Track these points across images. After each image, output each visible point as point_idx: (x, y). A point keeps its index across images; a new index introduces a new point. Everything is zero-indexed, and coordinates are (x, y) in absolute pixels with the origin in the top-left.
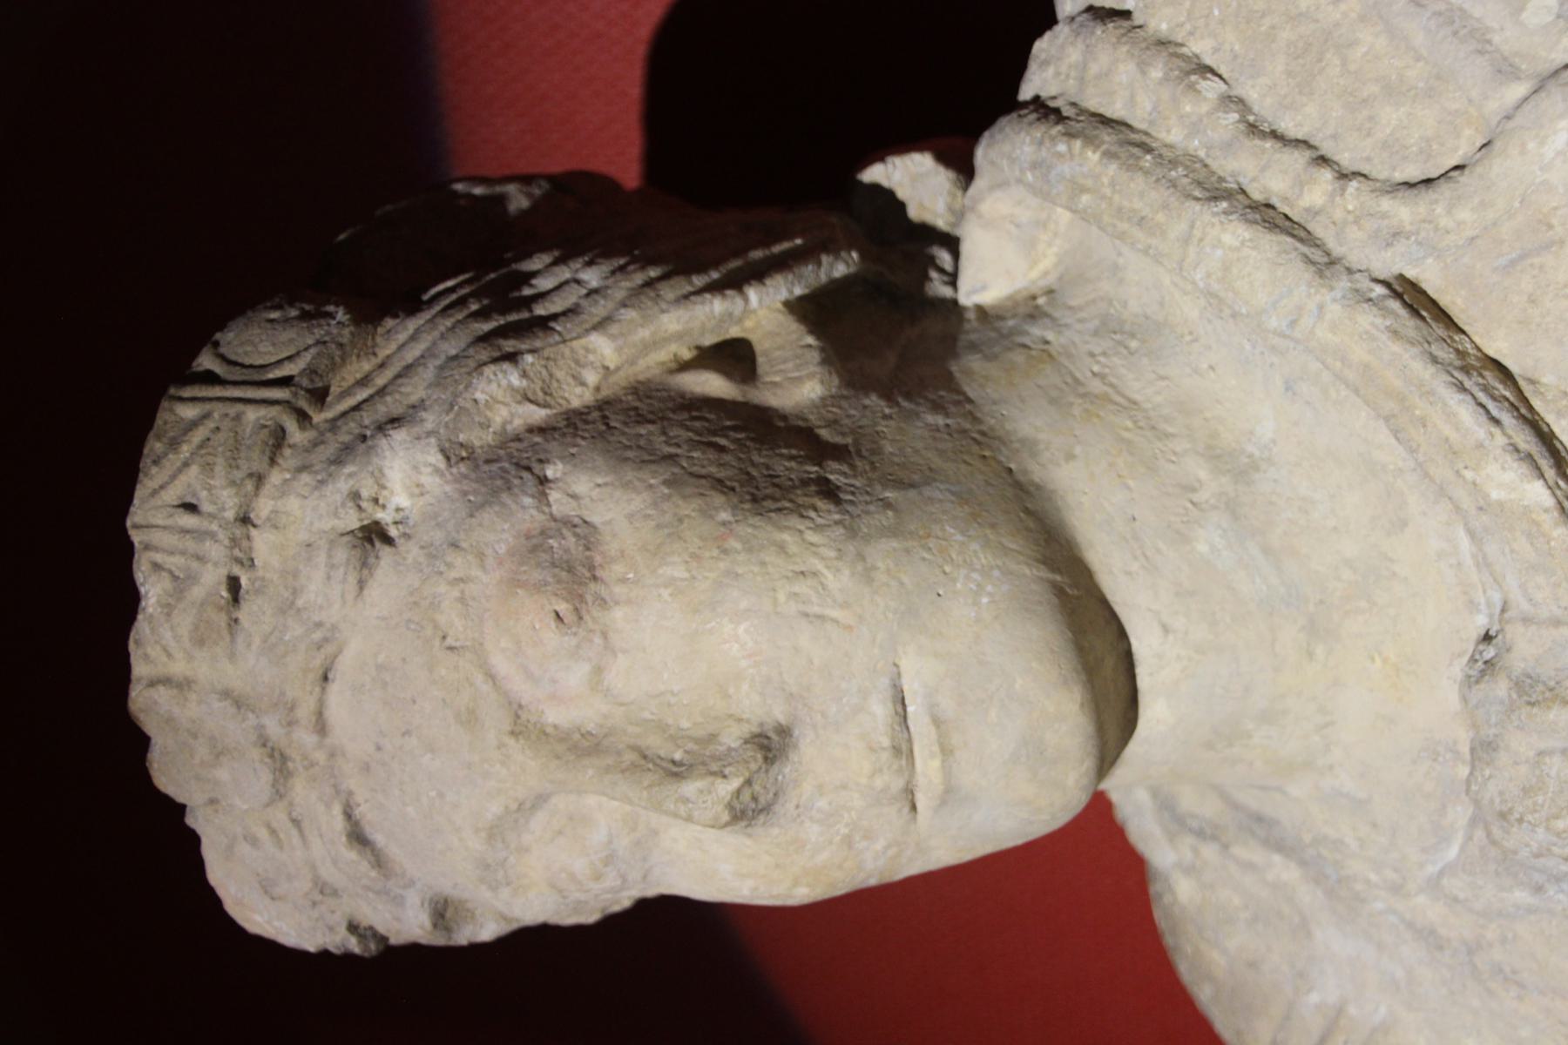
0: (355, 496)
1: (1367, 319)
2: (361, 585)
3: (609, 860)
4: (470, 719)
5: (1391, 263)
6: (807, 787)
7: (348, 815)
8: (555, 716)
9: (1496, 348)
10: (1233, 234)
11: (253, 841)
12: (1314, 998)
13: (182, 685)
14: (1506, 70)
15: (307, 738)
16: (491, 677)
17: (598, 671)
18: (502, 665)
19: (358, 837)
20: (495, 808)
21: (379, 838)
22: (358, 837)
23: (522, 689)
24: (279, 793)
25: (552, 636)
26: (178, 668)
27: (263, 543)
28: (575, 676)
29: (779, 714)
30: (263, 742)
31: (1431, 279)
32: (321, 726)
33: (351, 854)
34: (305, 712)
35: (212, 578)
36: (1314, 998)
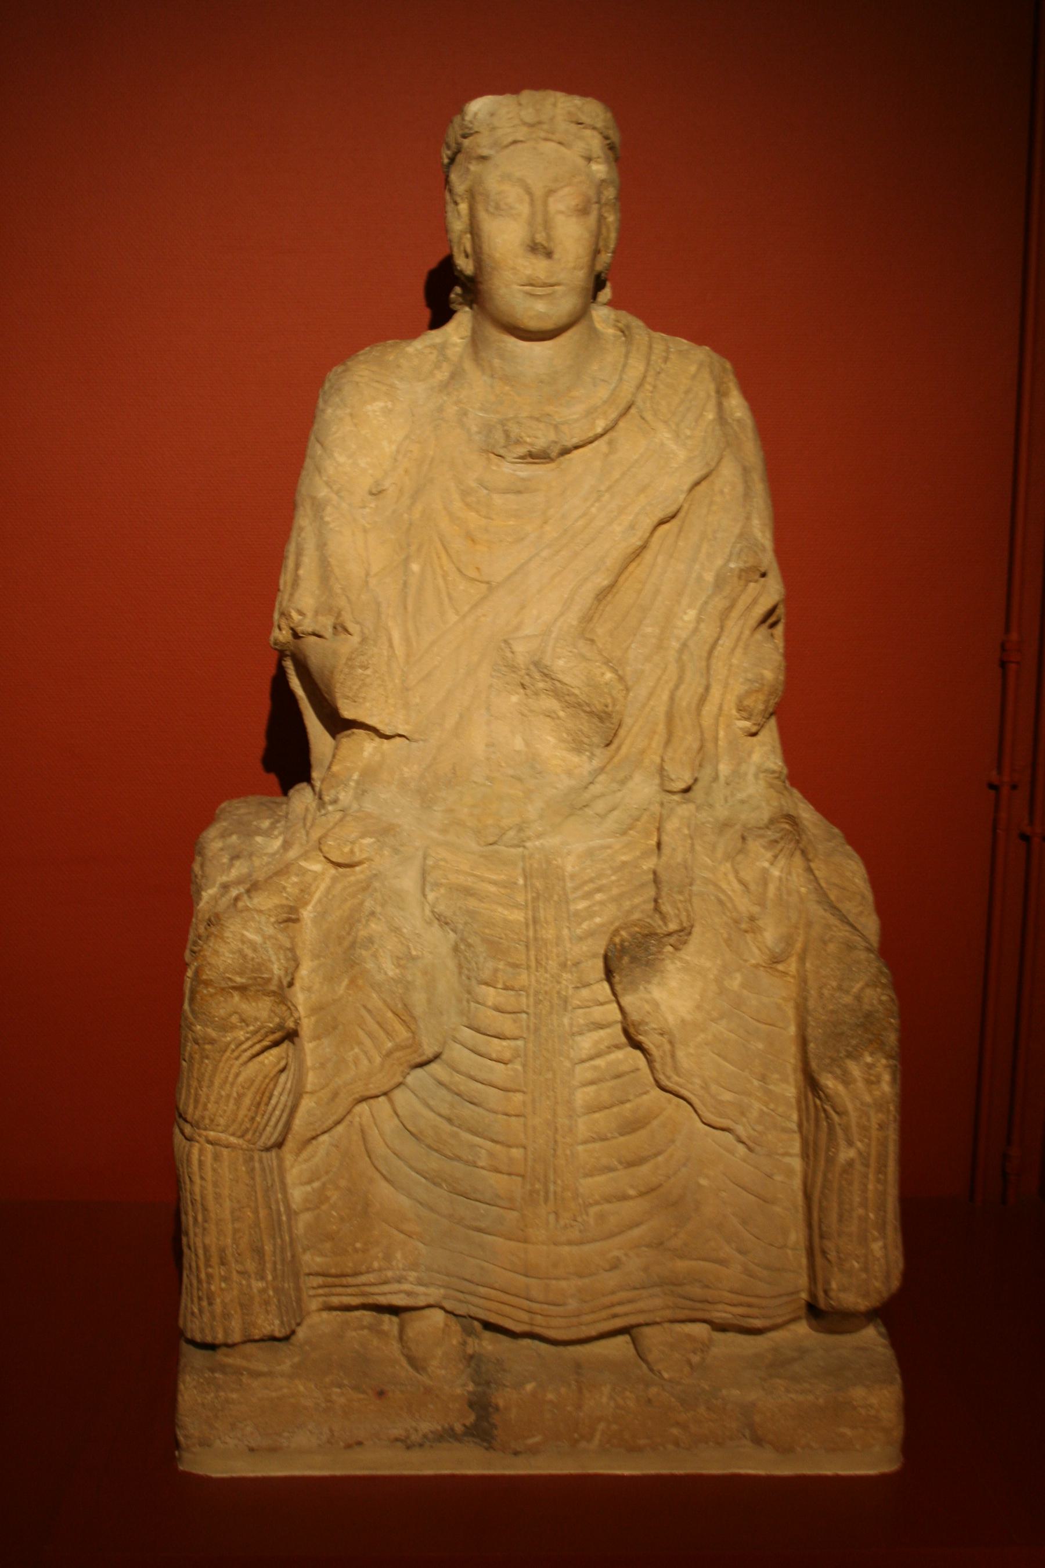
0: (598, 158)
1: (630, 396)
2: (582, 157)
3: (511, 208)
4: (556, 180)
5: (639, 402)
6: (535, 261)
7: (521, 141)
8: (551, 200)
9: (621, 424)
10: (642, 368)
11: (508, 113)
12: (397, 382)
13: (555, 105)
14: (677, 425)
15: (542, 134)
16: (562, 187)
17: (561, 212)
18: (566, 190)
19: (515, 142)
20: (529, 181)
21: (512, 147)
22: (515, 142)
23: (561, 193)
24: (525, 124)
25: (573, 203)
26: (560, 105)
27: (588, 133)
28: (561, 207)
29: (556, 256)
30: (540, 123)
31: (633, 411)
32: (546, 139)
33: (510, 139)
34: (550, 136)
35: (583, 118)
36: (397, 382)
